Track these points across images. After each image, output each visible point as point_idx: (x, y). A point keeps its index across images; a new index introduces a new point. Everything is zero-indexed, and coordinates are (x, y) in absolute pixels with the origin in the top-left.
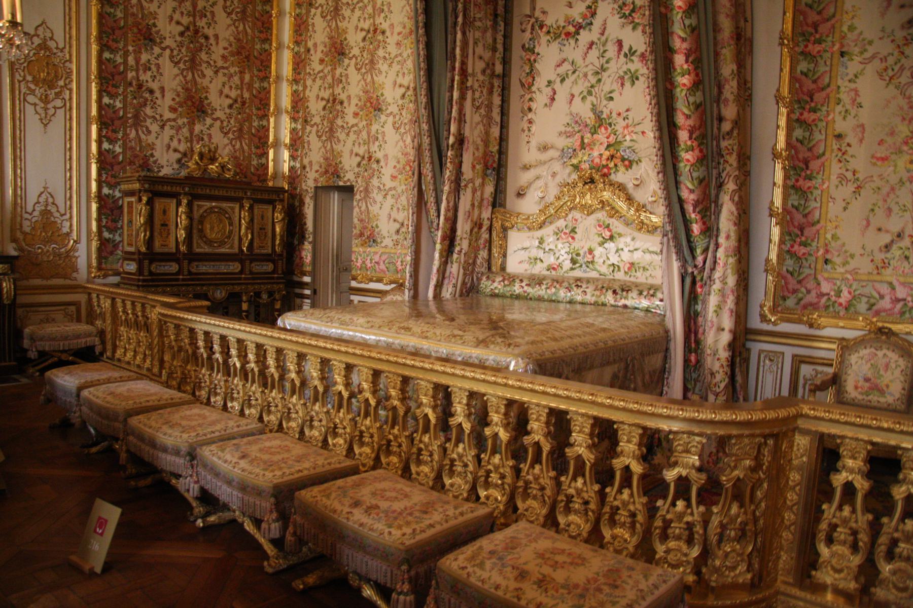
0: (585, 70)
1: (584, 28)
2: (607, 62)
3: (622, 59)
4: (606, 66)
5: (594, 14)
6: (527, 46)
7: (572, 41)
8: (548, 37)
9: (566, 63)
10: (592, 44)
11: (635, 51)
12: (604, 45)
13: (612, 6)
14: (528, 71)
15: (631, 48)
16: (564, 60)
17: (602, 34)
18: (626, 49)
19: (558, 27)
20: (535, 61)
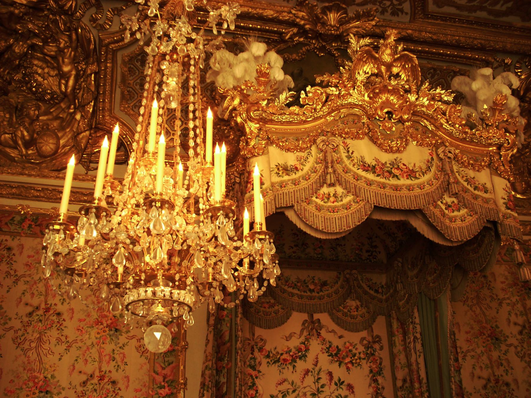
0: (305, 391)
1: (300, 358)
2: (323, 386)
3: (333, 387)
4: (321, 389)
5: (307, 349)
6: (248, 363)
7: (291, 368)
8: (268, 360)
9: (286, 383)
10: (307, 372)
11: (343, 382)
12: (318, 374)
13: (321, 346)
14: (250, 384)
15: (340, 380)
16: (285, 380)
17: (316, 365)
18: (336, 379)
19: (278, 353)
20: (257, 377)
